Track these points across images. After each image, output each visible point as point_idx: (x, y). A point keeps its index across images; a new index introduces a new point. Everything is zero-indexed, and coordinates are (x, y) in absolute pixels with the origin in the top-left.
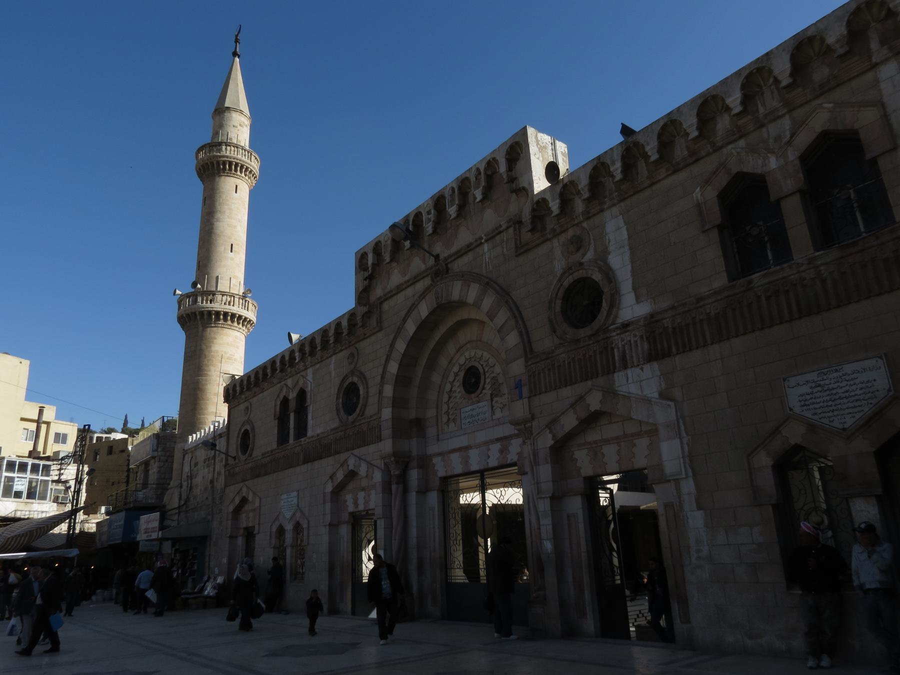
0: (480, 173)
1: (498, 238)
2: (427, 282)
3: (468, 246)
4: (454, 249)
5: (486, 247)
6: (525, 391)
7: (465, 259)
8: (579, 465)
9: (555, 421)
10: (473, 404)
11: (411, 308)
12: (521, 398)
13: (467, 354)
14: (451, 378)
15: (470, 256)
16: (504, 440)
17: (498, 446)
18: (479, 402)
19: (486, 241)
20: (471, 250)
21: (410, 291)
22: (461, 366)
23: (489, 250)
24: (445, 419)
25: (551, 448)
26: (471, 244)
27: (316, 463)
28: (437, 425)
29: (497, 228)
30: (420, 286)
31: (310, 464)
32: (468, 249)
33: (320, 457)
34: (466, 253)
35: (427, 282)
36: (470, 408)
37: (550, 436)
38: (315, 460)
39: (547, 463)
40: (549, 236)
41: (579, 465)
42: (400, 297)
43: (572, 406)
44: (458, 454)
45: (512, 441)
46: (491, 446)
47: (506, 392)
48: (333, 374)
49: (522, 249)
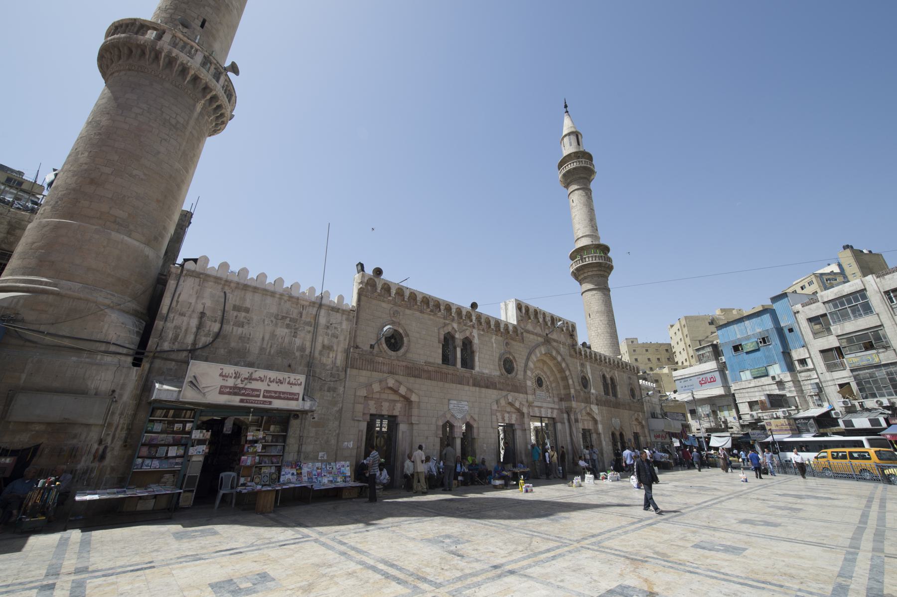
27: (483, 390)
33: (487, 387)
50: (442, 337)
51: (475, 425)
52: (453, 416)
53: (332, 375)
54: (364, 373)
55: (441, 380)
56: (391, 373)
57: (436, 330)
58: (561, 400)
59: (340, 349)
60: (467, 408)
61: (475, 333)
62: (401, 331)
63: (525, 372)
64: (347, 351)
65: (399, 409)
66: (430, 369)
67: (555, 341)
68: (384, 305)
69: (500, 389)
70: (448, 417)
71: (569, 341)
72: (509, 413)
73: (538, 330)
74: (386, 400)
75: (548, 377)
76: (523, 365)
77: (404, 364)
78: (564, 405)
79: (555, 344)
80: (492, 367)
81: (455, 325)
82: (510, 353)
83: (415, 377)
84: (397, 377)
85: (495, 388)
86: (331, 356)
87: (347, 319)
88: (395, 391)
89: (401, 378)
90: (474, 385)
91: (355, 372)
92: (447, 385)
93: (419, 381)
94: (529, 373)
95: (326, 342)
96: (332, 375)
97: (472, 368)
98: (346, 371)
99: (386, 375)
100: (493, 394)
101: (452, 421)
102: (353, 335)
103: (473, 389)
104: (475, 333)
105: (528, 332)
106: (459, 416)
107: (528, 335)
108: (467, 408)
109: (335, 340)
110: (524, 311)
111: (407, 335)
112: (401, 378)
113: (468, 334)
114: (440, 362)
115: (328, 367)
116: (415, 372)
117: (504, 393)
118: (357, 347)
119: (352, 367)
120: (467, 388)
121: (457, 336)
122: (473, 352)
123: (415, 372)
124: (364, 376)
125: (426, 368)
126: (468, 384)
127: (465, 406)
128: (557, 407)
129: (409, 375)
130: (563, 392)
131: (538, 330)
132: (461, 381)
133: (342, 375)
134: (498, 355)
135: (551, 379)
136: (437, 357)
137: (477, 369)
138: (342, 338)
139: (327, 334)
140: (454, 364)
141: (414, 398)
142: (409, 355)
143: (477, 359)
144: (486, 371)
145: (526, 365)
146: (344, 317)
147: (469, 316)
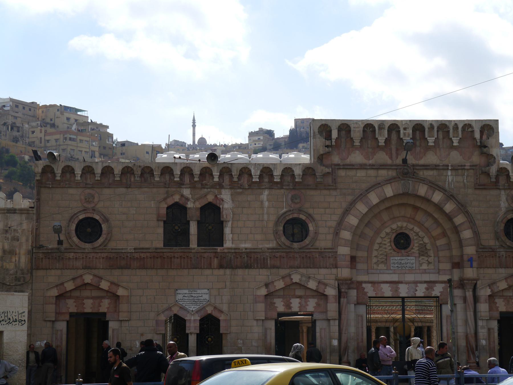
0: (457, 128)
1: (460, 171)
2: (392, 173)
3: (436, 166)
4: (422, 162)
5: (449, 173)
6: (475, 264)
7: (431, 173)
8: (497, 305)
9: (494, 283)
10: (402, 256)
11: (374, 186)
12: (471, 267)
13: (399, 224)
14: (383, 235)
15: (435, 173)
16: (431, 284)
17: (425, 285)
18: (408, 256)
19: (451, 170)
20: (436, 169)
21: (372, 173)
22: (392, 229)
23: (451, 175)
24: (374, 260)
25: (489, 296)
26: (439, 166)
27: (240, 272)
28: (367, 263)
29: (461, 166)
30: (383, 173)
31: (228, 271)
32: (435, 167)
33: (248, 266)
34: (432, 169)
35: (392, 173)
36: (399, 258)
37: (489, 290)
38: (237, 267)
39: (486, 303)
40: (501, 187)
41: (497, 305)
42: (361, 173)
43: (506, 279)
44: (388, 285)
45: (436, 285)
46: (418, 285)
47: (432, 255)
48: (266, 204)
49: (480, 187)
50: (164, 211)
51: (222, 318)
52: (182, 308)
53: (17, 279)
54: (53, 272)
55: (162, 268)
56: (85, 268)
57: (153, 204)
58: (457, 265)
59: (23, 251)
60: (207, 297)
61: (226, 195)
62: (97, 217)
63: (337, 234)
64: (30, 253)
65: (107, 305)
66: (142, 255)
67: (426, 167)
68: (71, 191)
69: (274, 267)
70: (175, 310)
71: (476, 159)
72: (300, 297)
73: (382, 157)
74: (88, 298)
75: (427, 231)
76: (334, 224)
77: (104, 255)
78: (456, 275)
79: (428, 174)
80: (258, 237)
81: (187, 192)
82: (300, 211)
83: (121, 268)
84: (95, 272)
85: (264, 266)
86: (14, 260)
87: (27, 218)
88: (98, 288)
89: (101, 273)
90: (221, 266)
91: (41, 273)
92: (172, 272)
93: (126, 272)
94: (346, 235)
95: (7, 247)
96: (17, 279)
97: (220, 242)
98: (31, 273)
99: (80, 272)
100: (261, 275)
101: (181, 314)
102: (36, 236)
103: (221, 272)
104: (226, 195)
105: (351, 167)
106: (193, 308)
107: (352, 173)
108: (207, 297)
109: (16, 243)
110: (335, 134)
111: (107, 220)
112: (101, 273)
113: (210, 198)
114: (161, 245)
115: (11, 272)
116: (120, 261)
117: (283, 272)
118: (41, 247)
119: (38, 269)
120: (208, 272)
121: (190, 205)
122: (221, 225)
123: (120, 261)
124: (52, 276)
125: (136, 255)
126: (210, 267)
127: (204, 295)
128: (446, 278)
129: (112, 267)
130: (455, 252)
131: (382, 157)
132: (196, 264)
133: (28, 277)
134: (273, 218)
135: (437, 232)
136: (155, 238)
137: (228, 244)
138: (23, 239)
139: (7, 239)
140: (187, 243)
141: (120, 292)
142: (112, 245)
143: (227, 230)
144: (243, 245)
145: (340, 224)
146: (24, 216)
147: (206, 172)
